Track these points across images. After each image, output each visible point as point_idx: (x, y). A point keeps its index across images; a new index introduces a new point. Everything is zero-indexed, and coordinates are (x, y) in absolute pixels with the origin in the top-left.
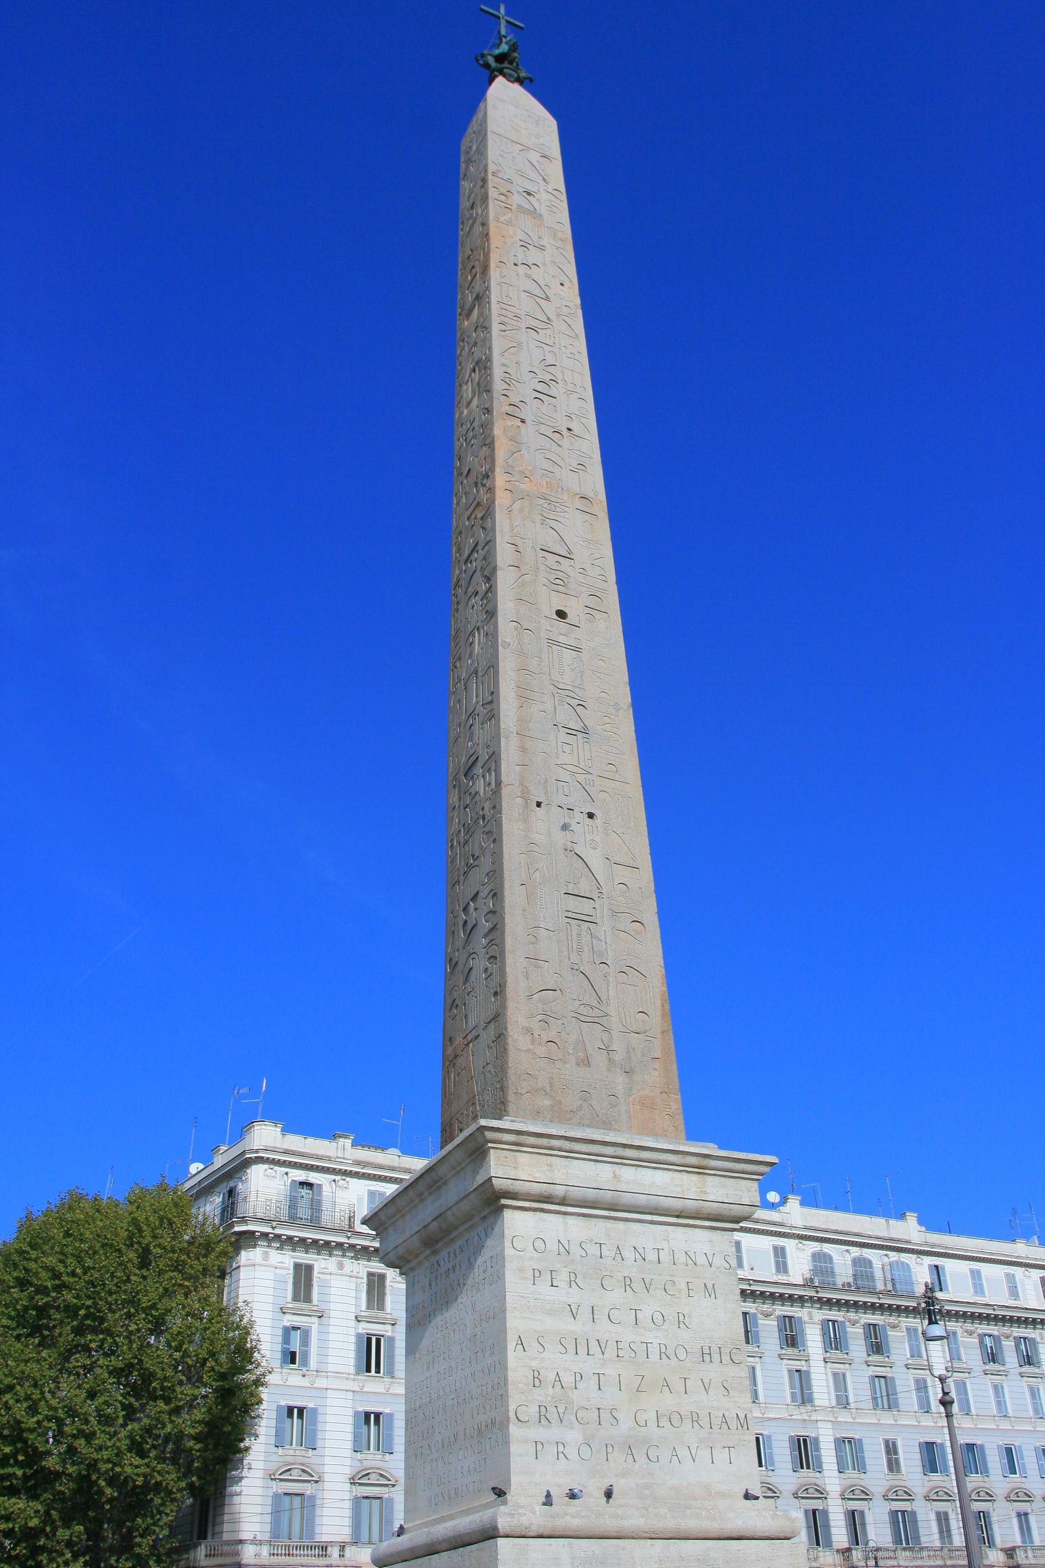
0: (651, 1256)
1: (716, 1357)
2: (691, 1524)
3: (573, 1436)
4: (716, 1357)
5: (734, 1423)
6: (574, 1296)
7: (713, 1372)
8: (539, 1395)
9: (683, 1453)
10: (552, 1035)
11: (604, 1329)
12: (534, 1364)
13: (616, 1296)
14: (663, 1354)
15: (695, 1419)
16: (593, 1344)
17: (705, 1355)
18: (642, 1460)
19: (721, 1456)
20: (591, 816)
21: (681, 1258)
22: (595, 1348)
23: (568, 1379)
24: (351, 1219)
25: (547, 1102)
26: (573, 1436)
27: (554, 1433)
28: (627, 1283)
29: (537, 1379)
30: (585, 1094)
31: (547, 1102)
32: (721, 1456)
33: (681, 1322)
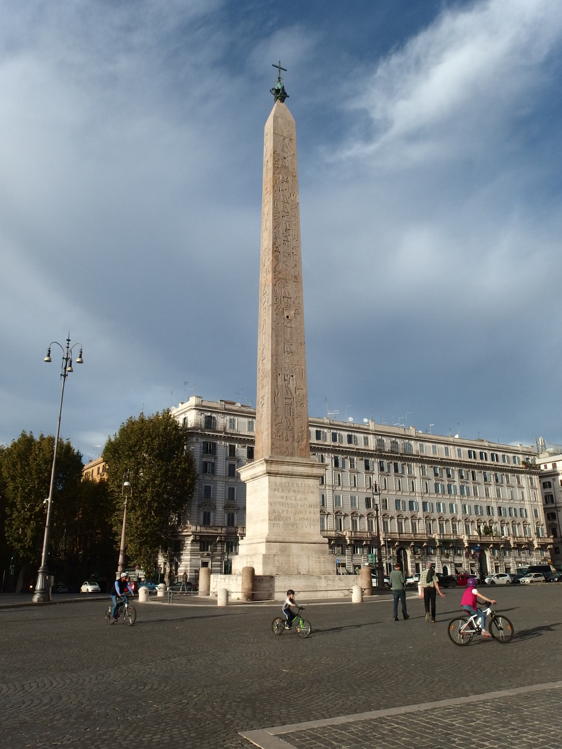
0: (300, 485)
1: (313, 507)
2: (304, 541)
3: (281, 523)
4: (313, 507)
5: (315, 520)
6: (283, 494)
7: (312, 510)
8: (274, 515)
9: (304, 526)
11: (289, 501)
12: (274, 508)
13: (292, 494)
14: (301, 506)
15: (307, 519)
16: (286, 504)
17: (310, 506)
18: (295, 527)
19: (312, 527)
21: (307, 485)
22: (286, 504)
23: (281, 511)
24: (225, 428)
26: (281, 523)
27: (278, 522)
28: (294, 491)
30: (287, 448)
32: (312, 527)
33: (306, 499)
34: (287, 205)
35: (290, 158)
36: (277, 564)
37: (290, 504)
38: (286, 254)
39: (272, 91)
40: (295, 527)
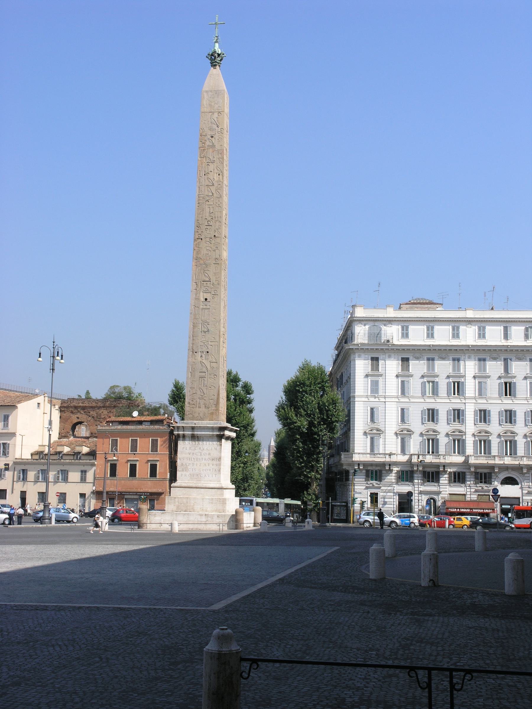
1: (215, 460)
4: (215, 460)
9: (207, 475)
10: (193, 403)
15: (210, 470)
16: (193, 459)
20: (208, 352)
22: (192, 459)
23: (188, 464)
25: (192, 416)
29: (182, 464)
31: (192, 416)
33: (209, 454)
34: (211, 187)
35: (217, 134)
36: (177, 503)
37: (196, 459)
38: (208, 240)
39: (208, 56)
40: (199, 476)
